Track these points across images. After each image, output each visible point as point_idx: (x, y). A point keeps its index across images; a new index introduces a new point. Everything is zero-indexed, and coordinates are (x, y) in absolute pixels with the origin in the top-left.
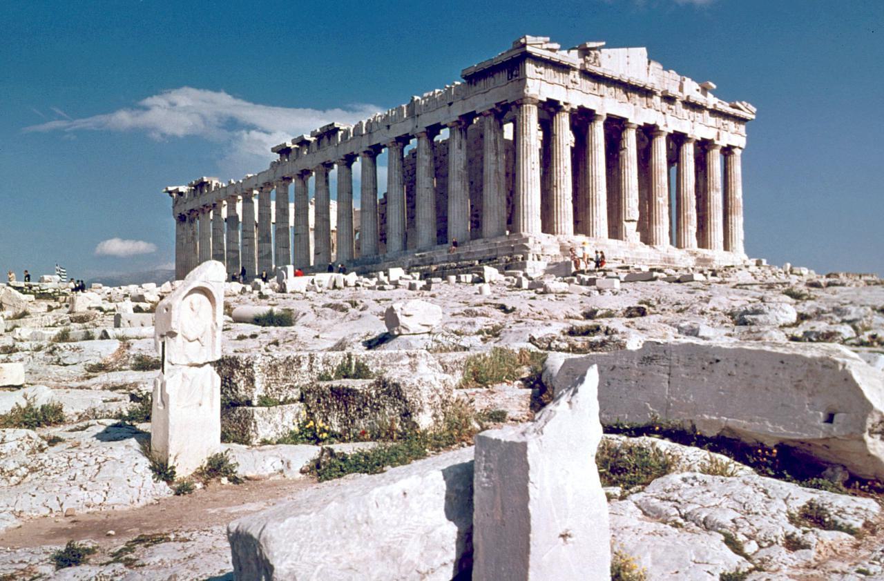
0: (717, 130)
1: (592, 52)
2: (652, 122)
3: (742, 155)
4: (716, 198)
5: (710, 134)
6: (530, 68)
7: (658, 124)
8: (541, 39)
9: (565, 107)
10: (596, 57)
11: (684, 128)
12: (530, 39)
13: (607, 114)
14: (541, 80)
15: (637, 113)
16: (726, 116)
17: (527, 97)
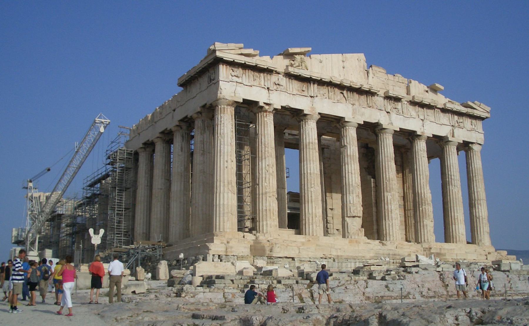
0: (451, 128)
1: (297, 56)
2: (373, 121)
3: (481, 152)
4: (457, 191)
5: (442, 132)
7: (382, 122)
8: (232, 45)
9: (267, 107)
10: (302, 61)
11: (411, 125)
13: (319, 114)
14: (237, 82)
15: (353, 112)
16: (460, 114)
17: (220, 99)
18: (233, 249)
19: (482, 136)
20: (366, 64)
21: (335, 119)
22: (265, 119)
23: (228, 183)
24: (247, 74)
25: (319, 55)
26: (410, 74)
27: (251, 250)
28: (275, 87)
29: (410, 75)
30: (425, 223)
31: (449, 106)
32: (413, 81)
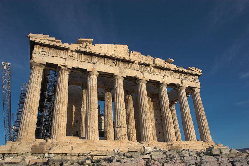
0: (180, 80)
5: (177, 81)
6: (36, 49)
7: (138, 77)
9: (63, 67)
12: (31, 35)
13: (98, 71)
18: (17, 149)
19: (199, 84)
20: (128, 50)
21: (110, 75)
22: (62, 74)
23: (29, 108)
24: (52, 51)
25: (100, 44)
26: (154, 55)
27: (32, 149)
28: (70, 58)
29: (154, 56)
30: (169, 130)
31: (178, 69)
32: (156, 58)
